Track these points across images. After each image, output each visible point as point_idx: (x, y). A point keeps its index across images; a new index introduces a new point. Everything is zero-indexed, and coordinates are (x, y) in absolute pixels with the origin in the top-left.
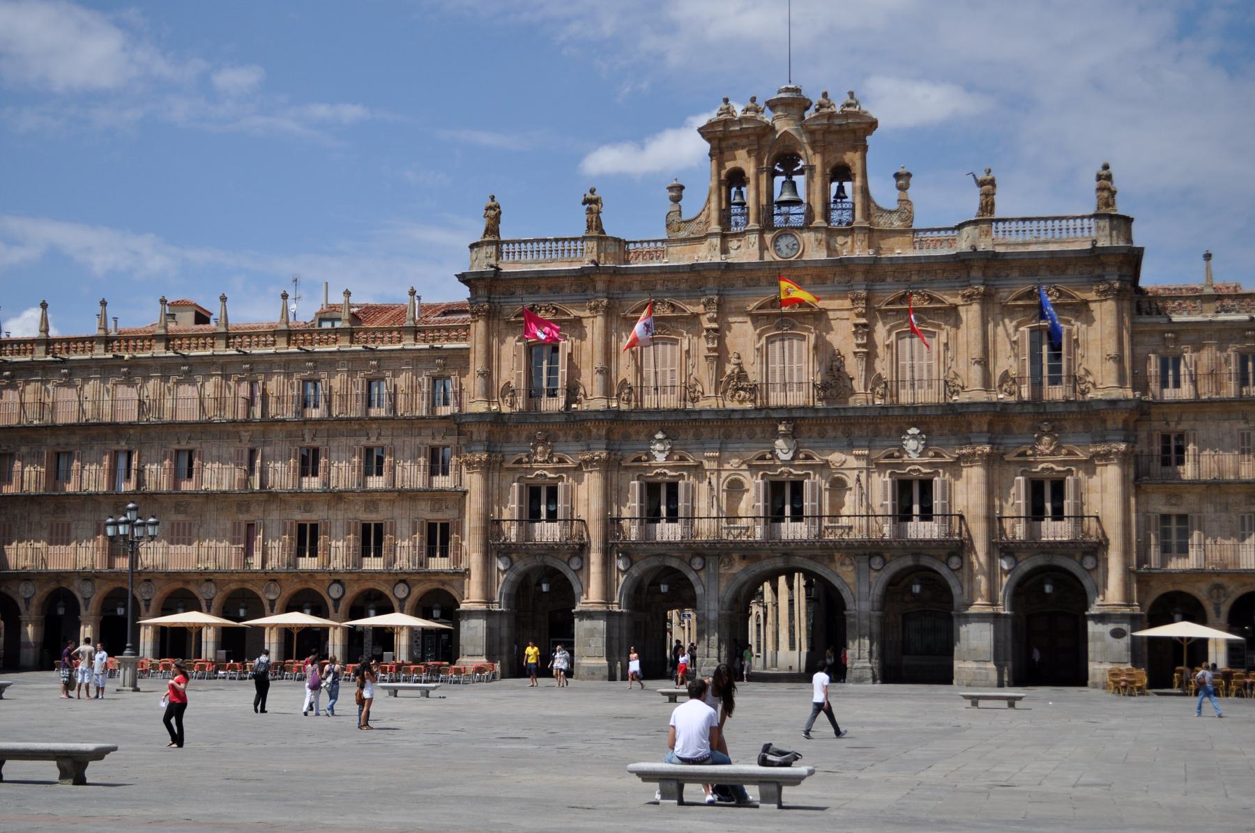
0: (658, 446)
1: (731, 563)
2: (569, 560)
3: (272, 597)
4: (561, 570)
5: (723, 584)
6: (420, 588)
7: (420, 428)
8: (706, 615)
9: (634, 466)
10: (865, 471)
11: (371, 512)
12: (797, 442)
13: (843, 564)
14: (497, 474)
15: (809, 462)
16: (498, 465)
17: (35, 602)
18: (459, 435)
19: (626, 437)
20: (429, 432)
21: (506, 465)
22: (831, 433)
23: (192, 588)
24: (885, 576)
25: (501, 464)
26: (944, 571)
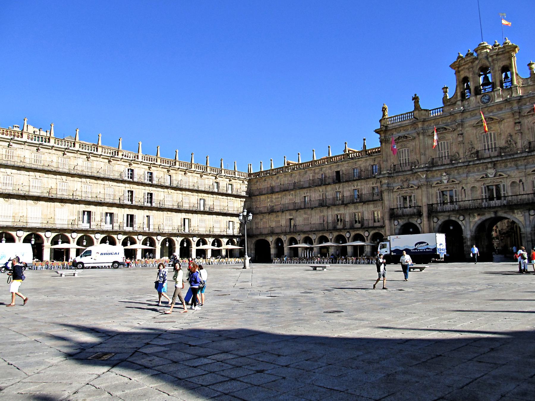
0: (444, 178)
1: (474, 217)
3: (331, 238)
5: (472, 225)
12: (496, 170)
13: (518, 214)
15: (501, 177)
17: (273, 242)
23: (310, 236)
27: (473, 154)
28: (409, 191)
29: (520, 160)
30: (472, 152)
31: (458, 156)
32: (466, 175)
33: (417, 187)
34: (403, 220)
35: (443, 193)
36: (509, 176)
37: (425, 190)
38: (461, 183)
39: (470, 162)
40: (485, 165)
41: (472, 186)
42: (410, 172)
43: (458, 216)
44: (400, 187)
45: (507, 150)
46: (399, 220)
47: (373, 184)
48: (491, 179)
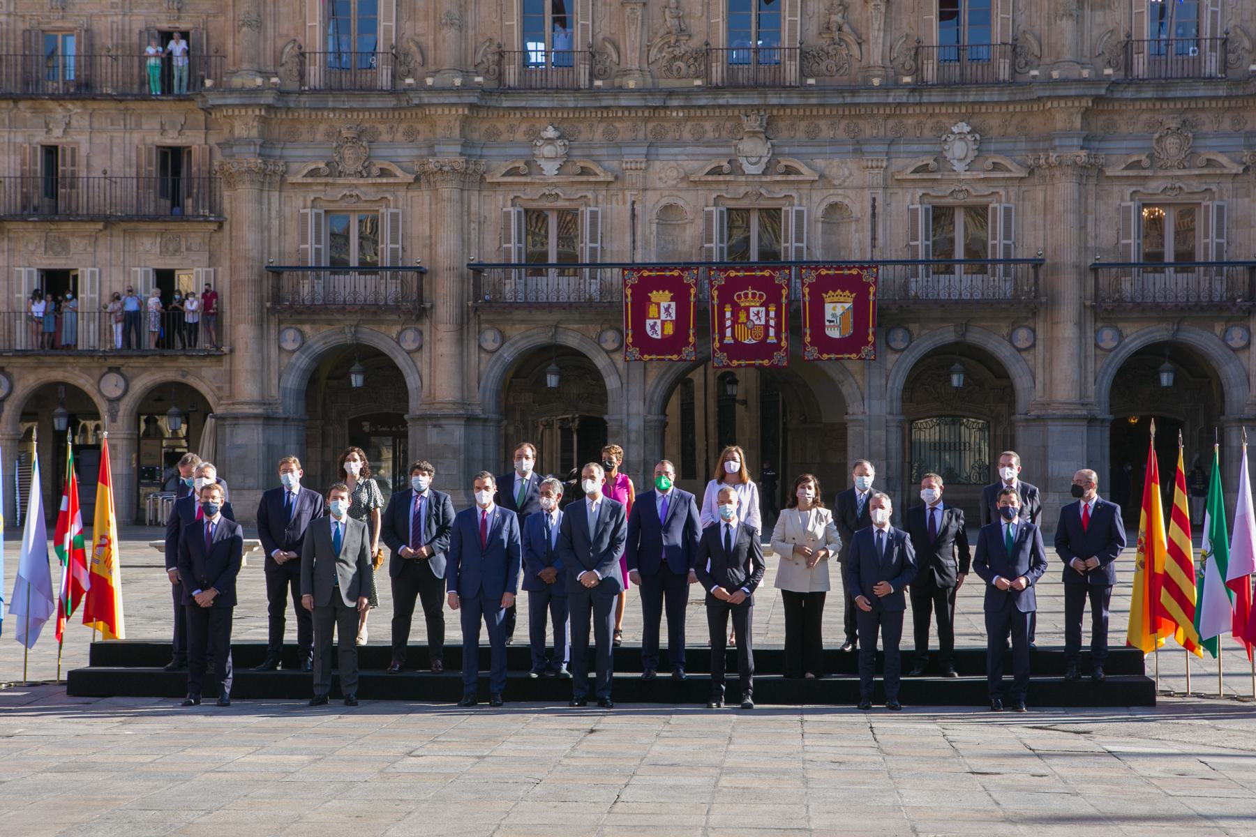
0: (548, 150)
2: (399, 334)
4: (385, 350)
6: (145, 381)
7: (140, 115)
8: (625, 421)
9: (505, 183)
10: (881, 191)
11: (57, 254)
12: (773, 145)
14: (277, 194)
15: (792, 178)
16: (278, 178)
18: (206, 129)
19: (493, 134)
20: (155, 123)
21: (291, 179)
22: (826, 131)
24: (910, 359)
25: (282, 176)
26: (1003, 351)
27: (681, 58)
28: (366, 190)
29: (872, 115)
30: (677, 52)
31: (615, 57)
32: (644, 150)
33: (410, 178)
34: (325, 329)
35: (534, 218)
36: (822, 176)
37: (456, 195)
38: (619, 185)
39: (671, 93)
40: (729, 118)
41: (664, 201)
42: (391, 102)
43: (593, 330)
44: (322, 165)
45: (823, 66)
46: (307, 328)
47: (163, 131)
48: (747, 183)
